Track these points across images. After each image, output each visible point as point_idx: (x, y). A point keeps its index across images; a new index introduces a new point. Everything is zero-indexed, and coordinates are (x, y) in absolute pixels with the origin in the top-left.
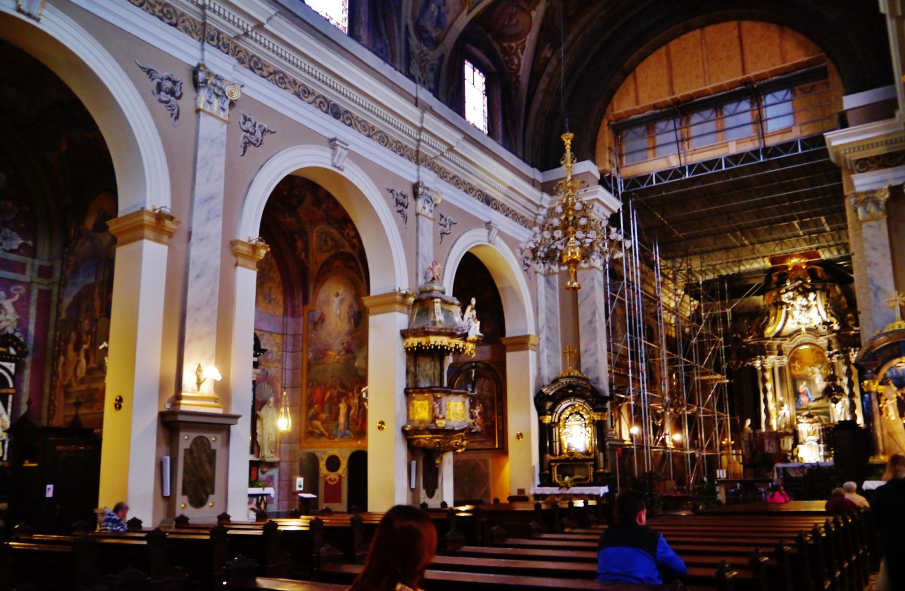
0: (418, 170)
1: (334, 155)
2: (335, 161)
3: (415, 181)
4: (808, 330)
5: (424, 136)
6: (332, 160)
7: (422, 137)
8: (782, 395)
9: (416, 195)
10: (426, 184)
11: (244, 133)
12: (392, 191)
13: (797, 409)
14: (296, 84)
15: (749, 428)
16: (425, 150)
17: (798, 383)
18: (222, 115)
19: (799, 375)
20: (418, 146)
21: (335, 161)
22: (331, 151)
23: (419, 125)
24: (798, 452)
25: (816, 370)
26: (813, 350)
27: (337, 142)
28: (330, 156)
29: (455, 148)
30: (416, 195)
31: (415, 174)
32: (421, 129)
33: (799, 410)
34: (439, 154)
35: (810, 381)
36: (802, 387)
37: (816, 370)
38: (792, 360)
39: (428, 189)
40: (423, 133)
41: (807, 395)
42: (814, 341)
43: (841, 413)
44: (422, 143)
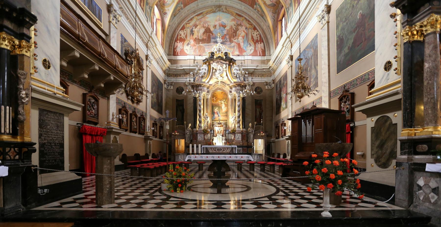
4: (221, 82)
8: (207, 112)
13: (212, 120)
15: (190, 128)
17: (214, 108)
19: (215, 104)
24: (213, 140)
25: (223, 102)
26: (222, 93)
33: (213, 119)
35: (220, 107)
36: (216, 110)
37: (223, 102)
38: (213, 96)
41: (218, 114)
42: (224, 89)
43: (233, 123)
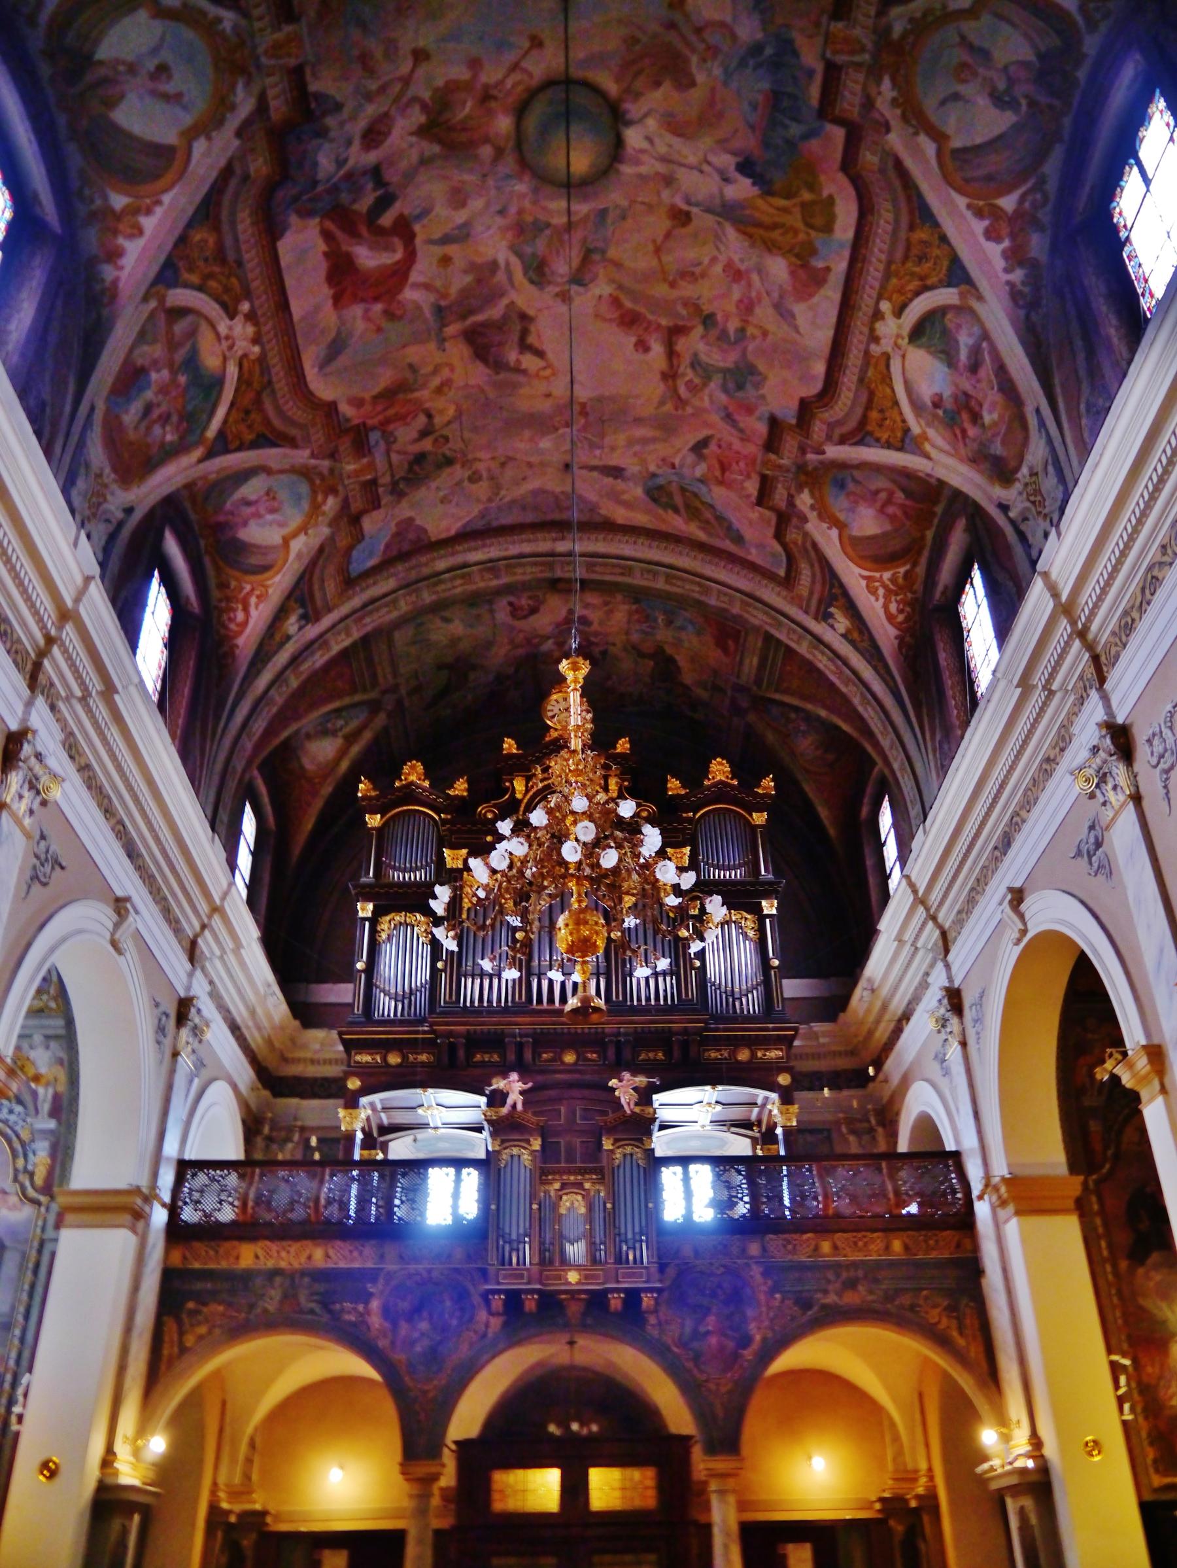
0: (191, 975)
1: (117, 926)
2: (117, 936)
3: (182, 994)
5: (217, 921)
6: (112, 935)
7: (213, 923)
9: (182, 1018)
10: (202, 1007)
11: (35, 860)
12: (157, 1005)
14: (101, 793)
16: (206, 943)
18: (27, 821)
20: (196, 936)
21: (117, 936)
22: (115, 917)
23: (218, 902)
27: (129, 906)
28: (110, 926)
29: (242, 951)
30: (182, 1018)
31: (184, 977)
32: (216, 909)
34: (218, 952)
39: (199, 1011)
40: (216, 917)
44: (207, 933)
